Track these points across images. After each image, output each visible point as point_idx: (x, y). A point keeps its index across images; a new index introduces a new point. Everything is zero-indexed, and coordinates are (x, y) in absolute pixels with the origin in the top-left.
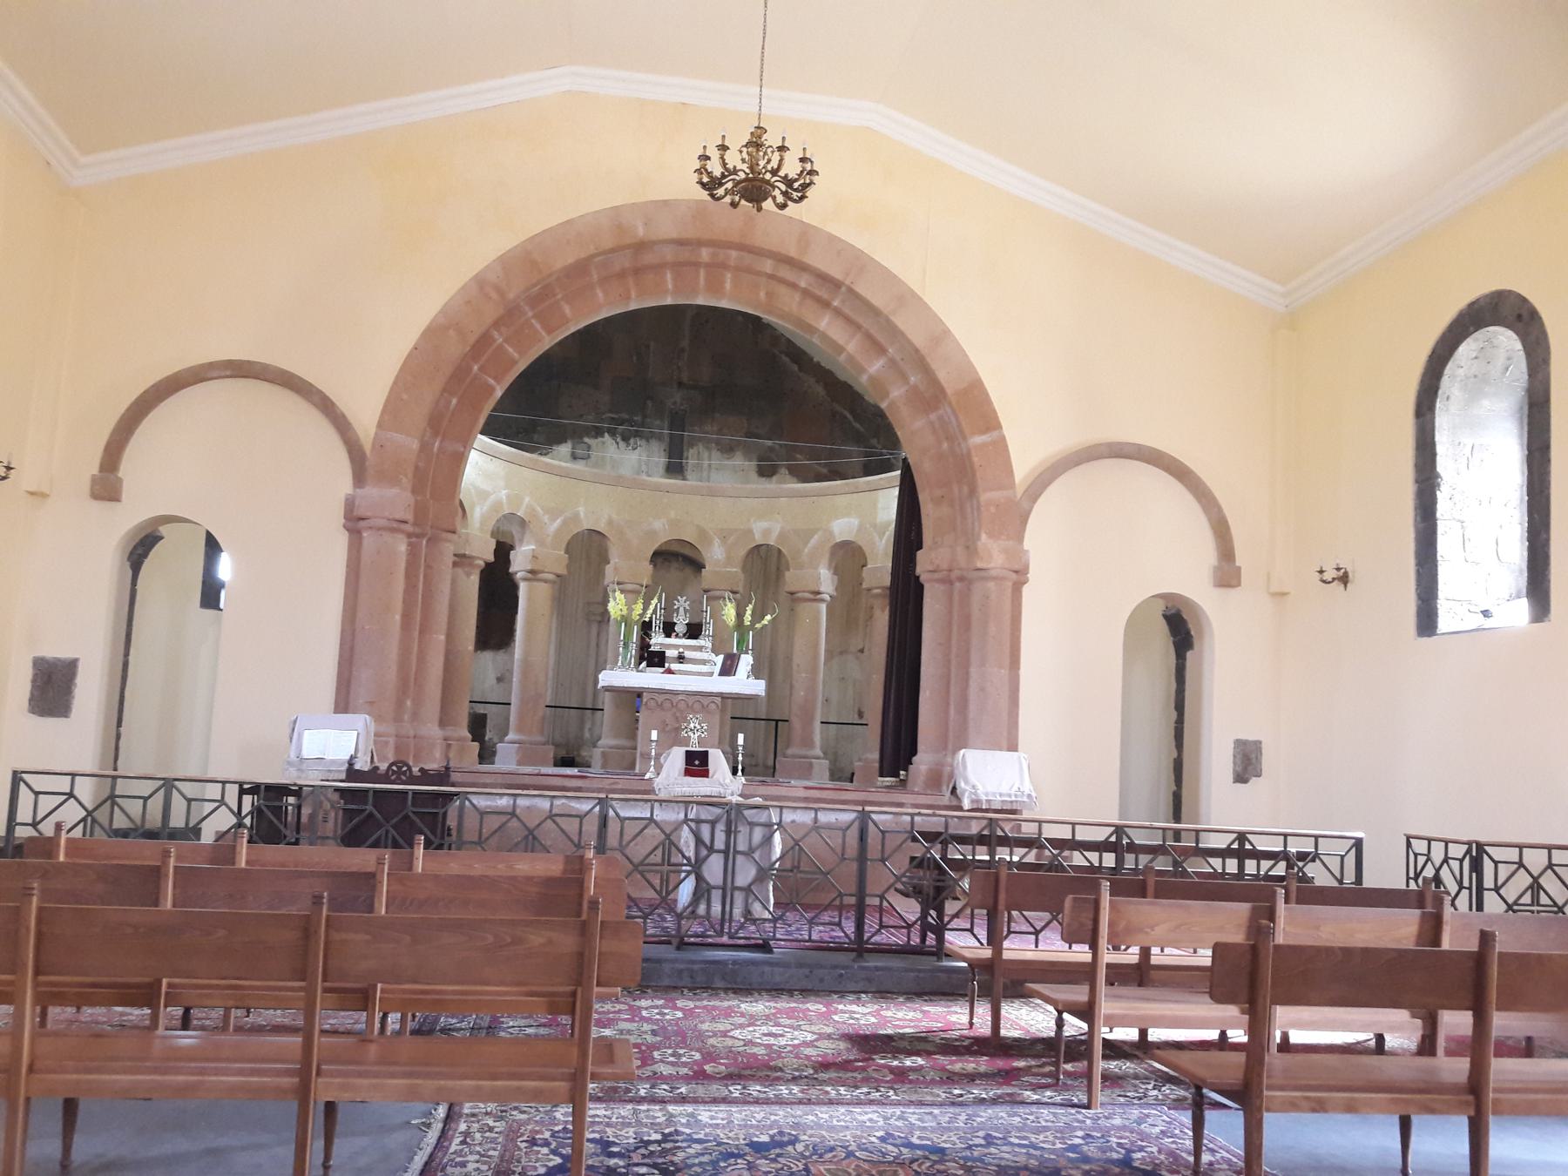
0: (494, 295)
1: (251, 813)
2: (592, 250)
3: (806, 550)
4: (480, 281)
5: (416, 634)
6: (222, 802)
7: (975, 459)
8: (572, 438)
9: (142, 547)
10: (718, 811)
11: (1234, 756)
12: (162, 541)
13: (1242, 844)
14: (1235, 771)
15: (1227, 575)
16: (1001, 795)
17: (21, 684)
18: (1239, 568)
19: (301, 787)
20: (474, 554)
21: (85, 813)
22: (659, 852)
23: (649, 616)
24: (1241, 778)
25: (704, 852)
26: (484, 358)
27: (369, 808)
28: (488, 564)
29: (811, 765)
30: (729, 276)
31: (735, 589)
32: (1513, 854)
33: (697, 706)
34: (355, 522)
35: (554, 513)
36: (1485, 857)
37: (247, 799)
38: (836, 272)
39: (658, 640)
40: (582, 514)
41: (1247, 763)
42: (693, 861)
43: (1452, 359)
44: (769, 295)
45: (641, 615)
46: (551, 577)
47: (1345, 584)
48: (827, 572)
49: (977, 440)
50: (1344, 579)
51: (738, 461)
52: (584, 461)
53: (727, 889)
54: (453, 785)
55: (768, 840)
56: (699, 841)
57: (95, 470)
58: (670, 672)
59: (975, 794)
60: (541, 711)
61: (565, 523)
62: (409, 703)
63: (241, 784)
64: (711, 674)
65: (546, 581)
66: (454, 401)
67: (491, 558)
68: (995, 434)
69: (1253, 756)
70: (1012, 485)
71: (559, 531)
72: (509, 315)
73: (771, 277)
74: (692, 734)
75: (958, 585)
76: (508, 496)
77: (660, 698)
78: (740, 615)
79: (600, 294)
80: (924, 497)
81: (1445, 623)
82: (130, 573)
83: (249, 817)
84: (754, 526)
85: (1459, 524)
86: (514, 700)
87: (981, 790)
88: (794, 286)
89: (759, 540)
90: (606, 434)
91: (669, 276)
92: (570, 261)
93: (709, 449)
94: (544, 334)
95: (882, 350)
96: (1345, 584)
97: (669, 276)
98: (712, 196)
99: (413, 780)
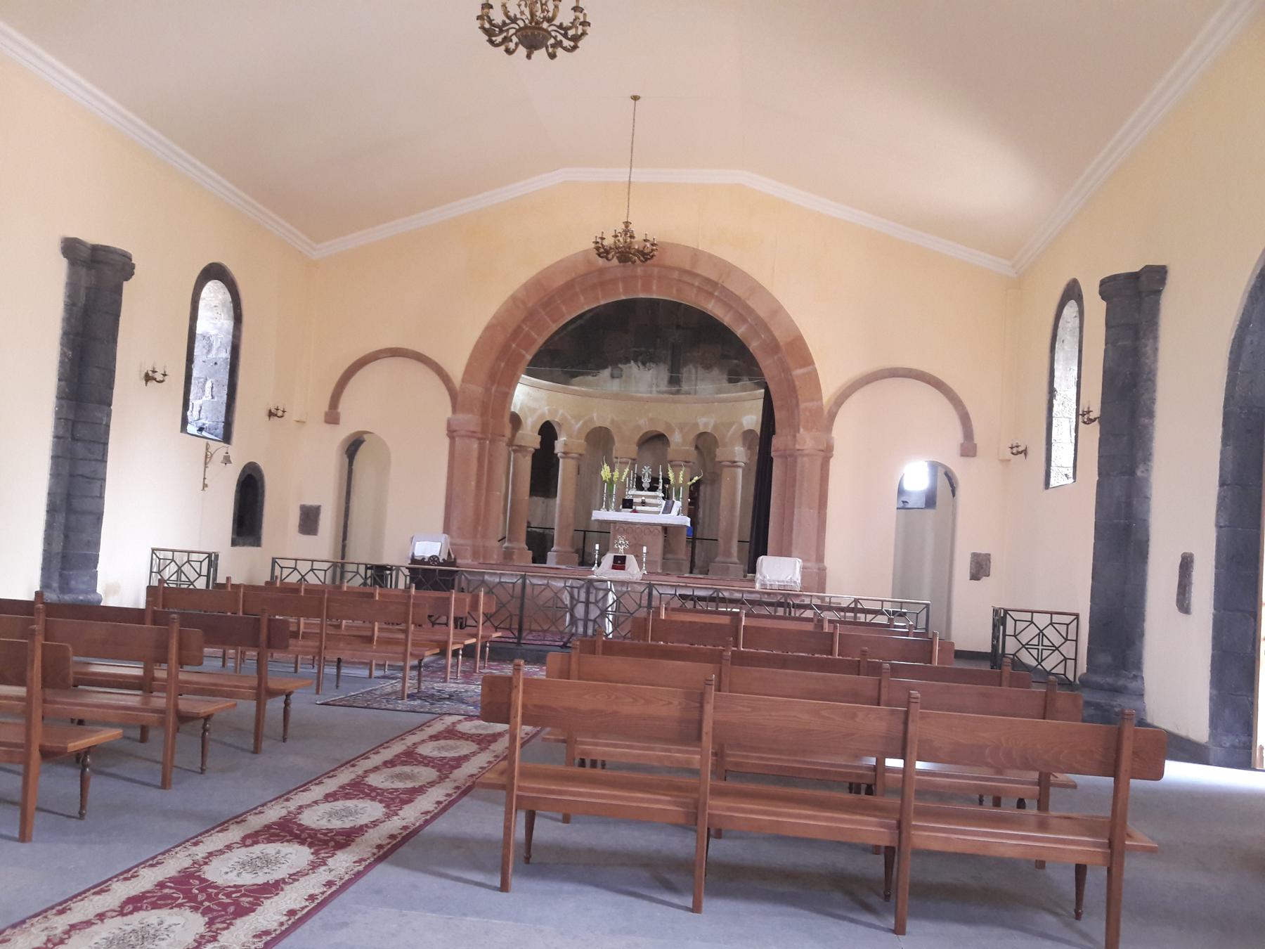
4: (513, 298)
6: (357, 573)
8: (611, 365)
9: (353, 447)
10: (582, 582)
12: (364, 444)
13: (856, 605)
14: (971, 572)
15: (969, 449)
16: (778, 581)
17: (294, 518)
18: (975, 445)
19: (392, 567)
21: (300, 577)
22: (552, 600)
23: (623, 478)
24: (975, 577)
25: (575, 602)
27: (420, 576)
28: (536, 450)
29: (728, 568)
30: (655, 282)
31: (687, 460)
32: (1028, 616)
33: (647, 531)
34: (452, 433)
35: (577, 418)
36: (1008, 615)
37: (369, 572)
38: (714, 277)
39: (632, 493)
41: (980, 567)
42: (569, 606)
45: (620, 478)
46: (576, 455)
47: (1026, 455)
48: (742, 449)
50: (1025, 452)
51: (715, 372)
53: (586, 620)
54: (457, 567)
55: (606, 596)
56: (572, 597)
58: (635, 511)
60: (571, 533)
61: (585, 423)
63: (366, 565)
65: (573, 458)
66: (503, 365)
67: (538, 446)
68: (810, 368)
69: (984, 563)
70: (821, 398)
71: (580, 429)
72: (531, 315)
74: (619, 546)
76: (549, 410)
78: (676, 477)
79: (582, 299)
80: (776, 403)
81: (1053, 483)
82: (347, 460)
83: (370, 579)
84: (699, 421)
85: (1068, 420)
86: (556, 528)
87: (768, 578)
88: (692, 285)
89: (702, 429)
90: (632, 362)
92: (561, 283)
93: (696, 368)
95: (744, 320)
96: (1026, 455)
98: (608, 259)
99: (440, 564)
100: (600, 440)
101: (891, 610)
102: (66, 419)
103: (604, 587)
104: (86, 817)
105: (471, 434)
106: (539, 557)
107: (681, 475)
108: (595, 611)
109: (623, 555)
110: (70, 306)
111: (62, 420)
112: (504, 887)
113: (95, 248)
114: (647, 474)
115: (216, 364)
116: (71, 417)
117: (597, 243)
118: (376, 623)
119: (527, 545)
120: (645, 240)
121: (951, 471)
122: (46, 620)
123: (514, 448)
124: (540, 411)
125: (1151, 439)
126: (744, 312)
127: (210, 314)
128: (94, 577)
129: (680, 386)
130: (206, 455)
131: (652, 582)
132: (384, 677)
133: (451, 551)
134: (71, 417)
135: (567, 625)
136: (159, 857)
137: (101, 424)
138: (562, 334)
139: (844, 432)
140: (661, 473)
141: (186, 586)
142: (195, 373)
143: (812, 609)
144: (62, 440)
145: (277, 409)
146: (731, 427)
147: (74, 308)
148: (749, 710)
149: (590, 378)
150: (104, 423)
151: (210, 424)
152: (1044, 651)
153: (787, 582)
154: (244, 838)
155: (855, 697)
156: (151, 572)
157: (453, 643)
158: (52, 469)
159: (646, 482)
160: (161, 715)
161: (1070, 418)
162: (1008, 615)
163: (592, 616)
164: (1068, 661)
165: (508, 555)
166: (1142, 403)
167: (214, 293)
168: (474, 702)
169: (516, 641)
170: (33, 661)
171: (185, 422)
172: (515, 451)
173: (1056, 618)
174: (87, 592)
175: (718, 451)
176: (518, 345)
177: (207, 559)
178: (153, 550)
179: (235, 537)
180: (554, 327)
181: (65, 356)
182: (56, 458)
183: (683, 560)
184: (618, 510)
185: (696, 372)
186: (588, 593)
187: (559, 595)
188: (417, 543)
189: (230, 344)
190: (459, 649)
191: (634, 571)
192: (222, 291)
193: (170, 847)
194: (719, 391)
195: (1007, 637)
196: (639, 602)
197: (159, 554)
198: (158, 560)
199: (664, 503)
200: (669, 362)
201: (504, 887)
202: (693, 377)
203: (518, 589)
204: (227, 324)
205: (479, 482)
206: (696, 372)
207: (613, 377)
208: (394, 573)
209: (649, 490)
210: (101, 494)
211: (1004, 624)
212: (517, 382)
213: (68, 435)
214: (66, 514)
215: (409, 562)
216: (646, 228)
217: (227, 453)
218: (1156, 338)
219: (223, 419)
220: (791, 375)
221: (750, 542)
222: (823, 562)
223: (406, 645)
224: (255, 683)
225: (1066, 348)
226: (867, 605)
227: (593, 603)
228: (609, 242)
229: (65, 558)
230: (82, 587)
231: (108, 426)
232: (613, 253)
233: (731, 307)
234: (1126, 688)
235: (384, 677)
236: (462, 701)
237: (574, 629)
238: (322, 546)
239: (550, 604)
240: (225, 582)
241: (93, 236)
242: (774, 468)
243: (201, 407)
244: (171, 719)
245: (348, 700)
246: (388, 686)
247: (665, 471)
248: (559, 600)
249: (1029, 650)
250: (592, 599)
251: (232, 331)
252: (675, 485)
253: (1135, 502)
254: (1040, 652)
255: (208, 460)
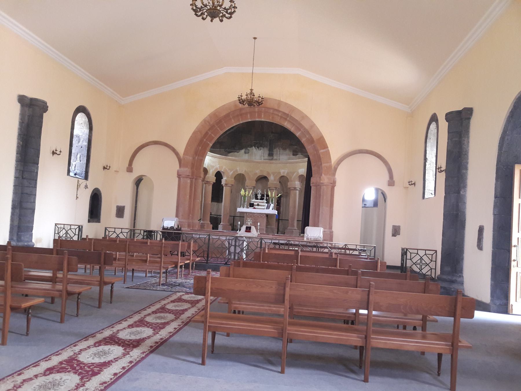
0: (208, 124)
1: (146, 235)
2: (229, 111)
3: (293, 177)
4: (205, 121)
5: (192, 200)
6: (140, 233)
7: (321, 156)
8: (245, 148)
9: (138, 182)
10: (233, 237)
11: (392, 230)
13: (346, 247)
14: (392, 233)
15: (391, 183)
16: (314, 237)
17: (114, 211)
18: (394, 182)
19: (155, 231)
20: (210, 181)
21: (117, 235)
22: (221, 245)
23: (250, 195)
24: (394, 235)
26: (206, 138)
27: (166, 235)
28: (214, 183)
29: (293, 231)
30: (263, 114)
31: (276, 187)
32: (416, 251)
33: (260, 216)
34: (179, 176)
36: (408, 251)
37: (145, 233)
38: (287, 112)
39: (254, 201)
40: (238, 170)
41: (396, 231)
42: (228, 247)
43: (430, 129)
44: (273, 118)
46: (230, 185)
48: (299, 182)
49: (322, 151)
50: (414, 184)
51: (288, 151)
52: (248, 154)
53: (235, 253)
54: (182, 231)
55: (243, 243)
56: (229, 243)
57: (127, 166)
58: (255, 208)
59: (307, 237)
60: (228, 217)
61: (234, 172)
62: (191, 215)
63: (144, 230)
64: (264, 209)
65: (229, 186)
66: (200, 148)
68: (326, 149)
70: (331, 162)
71: (232, 174)
72: (212, 127)
73: (273, 113)
74: (248, 223)
75: (318, 187)
76: (219, 167)
77: (251, 215)
78: (272, 194)
79: (233, 120)
80: (313, 164)
81: (426, 196)
83: (145, 236)
87: (309, 235)
88: (278, 115)
90: (253, 147)
91: (249, 115)
92: (224, 114)
93: (280, 150)
94: (220, 131)
95: (300, 130)
97: (249, 115)
98: (243, 104)
100: (240, 179)
101: (360, 249)
102: (19, 170)
103: (242, 239)
104: (29, 335)
105: (187, 176)
106: (215, 227)
107: (274, 193)
108: (238, 250)
109: (250, 226)
110: (21, 123)
111: (18, 170)
112: (203, 363)
113: (32, 99)
114: (259, 193)
115: (82, 147)
116: (22, 169)
117: (239, 98)
118: (148, 254)
119: (210, 222)
120: (259, 97)
121: (384, 192)
122: (12, 253)
123: (205, 182)
124: (215, 167)
125: (466, 179)
126: (299, 126)
127: (79, 127)
128: (31, 235)
129: (273, 157)
130: (78, 185)
131: (262, 237)
132: (151, 277)
133: (179, 225)
134: (22, 169)
135: (227, 255)
136: (60, 351)
137: (34, 172)
138: (225, 135)
139: (341, 176)
140: (265, 193)
141: (69, 239)
142: (73, 151)
143: (328, 248)
144: (18, 179)
145: (107, 166)
146: (295, 173)
147: (23, 124)
148: (304, 290)
149: (236, 153)
150: (36, 171)
151: (79, 172)
152: (422, 266)
153: (317, 237)
154: (95, 344)
155: (347, 285)
156: (55, 233)
157: (180, 263)
158: (13, 190)
159: (259, 196)
160: (60, 293)
161: (433, 170)
162: (408, 251)
163: (237, 252)
164: (432, 270)
165: (202, 226)
166: (463, 164)
167: (81, 118)
168: (189, 287)
169: (206, 262)
170: (7, 271)
171: (69, 171)
172: (205, 183)
173: (427, 252)
174: (28, 242)
175: (289, 184)
176: (206, 140)
177: (78, 228)
178: (56, 224)
179: (89, 219)
180: (222, 132)
181: (19, 144)
182: (15, 186)
183: (274, 228)
184: (247, 208)
185: (280, 151)
186: (236, 242)
187: (223, 243)
188: (165, 221)
189: (88, 139)
190: (182, 265)
191: (254, 233)
192: (84, 117)
193: (64, 347)
194: (289, 159)
195: (407, 260)
196: (256, 246)
197: (59, 226)
198: (58, 228)
199: (266, 205)
200: (269, 147)
201: (203, 363)
202: (279, 153)
203: (207, 241)
204: (87, 131)
205: (190, 196)
206: (280, 151)
207: (245, 153)
208: (156, 234)
209: (260, 199)
210: (34, 201)
211: (406, 254)
212: (206, 155)
213: (21, 177)
214: (20, 209)
215: (162, 229)
216: (259, 92)
217: (86, 184)
218: (468, 138)
219: (85, 170)
220: (319, 152)
221: (302, 221)
222: (332, 229)
223: (161, 264)
224: (99, 279)
225: (431, 141)
226: (350, 247)
227: (237, 246)
228: (244, 97)
229: (19, 227)
230: (27, 239)
231: (37, 173)
232: (246, 102)
233: (294, 125)
234: (456, 281)
235: (151, 277)
236: (184, 287)
237: (230, 256)
238: (125, 222)
239: (220, 246)
240: (86, 237)
241: (31, 94)
242: (312, 190)
243: (75, 165)
244: (64, 293)
245: (137, 286)
246: (153, 281)
247: (267, 192)
248: (224, 245)
249: (417, 265)
250: (237, 244)
251: (88, 133)
252: (271, 197)
253: (460, 205)
254: (421, 266)
255: (78, 187)
